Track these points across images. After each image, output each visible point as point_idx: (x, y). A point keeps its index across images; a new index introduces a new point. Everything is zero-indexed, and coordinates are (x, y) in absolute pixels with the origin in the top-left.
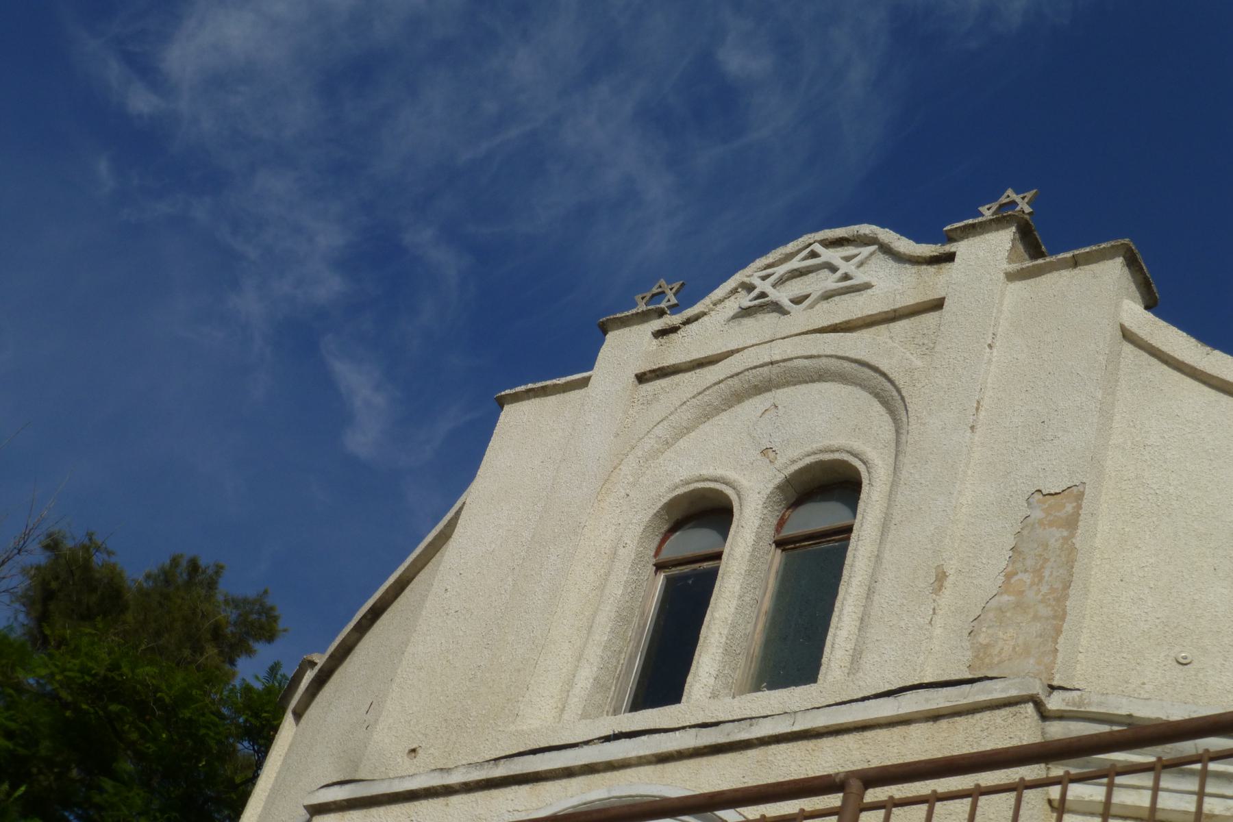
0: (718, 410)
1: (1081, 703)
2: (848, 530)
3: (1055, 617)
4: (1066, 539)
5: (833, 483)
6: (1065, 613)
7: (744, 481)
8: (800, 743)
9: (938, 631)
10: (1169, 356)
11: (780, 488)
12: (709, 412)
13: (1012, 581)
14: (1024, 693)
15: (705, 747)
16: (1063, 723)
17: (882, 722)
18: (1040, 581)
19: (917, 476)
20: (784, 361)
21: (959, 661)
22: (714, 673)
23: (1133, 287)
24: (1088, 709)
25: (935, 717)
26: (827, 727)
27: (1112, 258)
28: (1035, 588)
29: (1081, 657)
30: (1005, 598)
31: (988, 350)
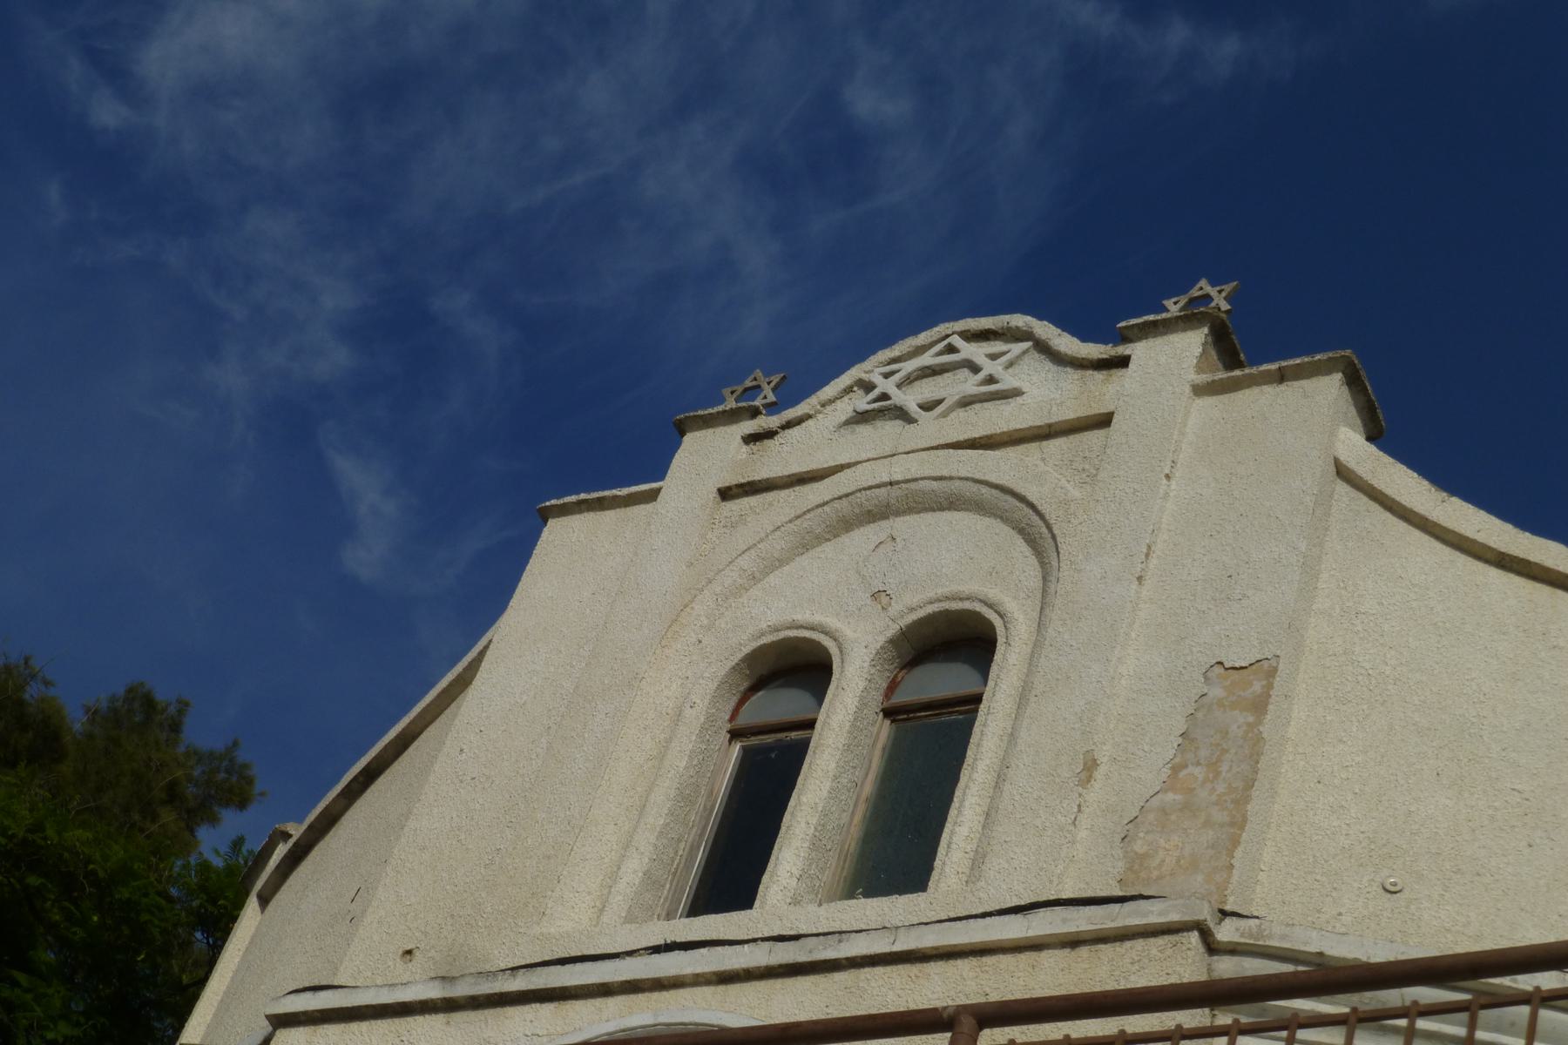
0: (820, 540)
2: (977, 699)
3: (1232, 824)
6: (1245, 820)
7: (848, 631)
8: (900, 967)
9: (1083, 834)
10: (1393, 500)
11: (892, 641)
12: (807, 543)
13: (1182, 774)
14: (1187, 918)
15: (781, 966)
16: (1236, 959)
22: (797, 873)
23: (1353, 411)
24: (1268, 943)
25: (1073, 942)
27: (1329, 372)
29: (1262, 876)
30: (1170, 796)
31: (1165, 481)
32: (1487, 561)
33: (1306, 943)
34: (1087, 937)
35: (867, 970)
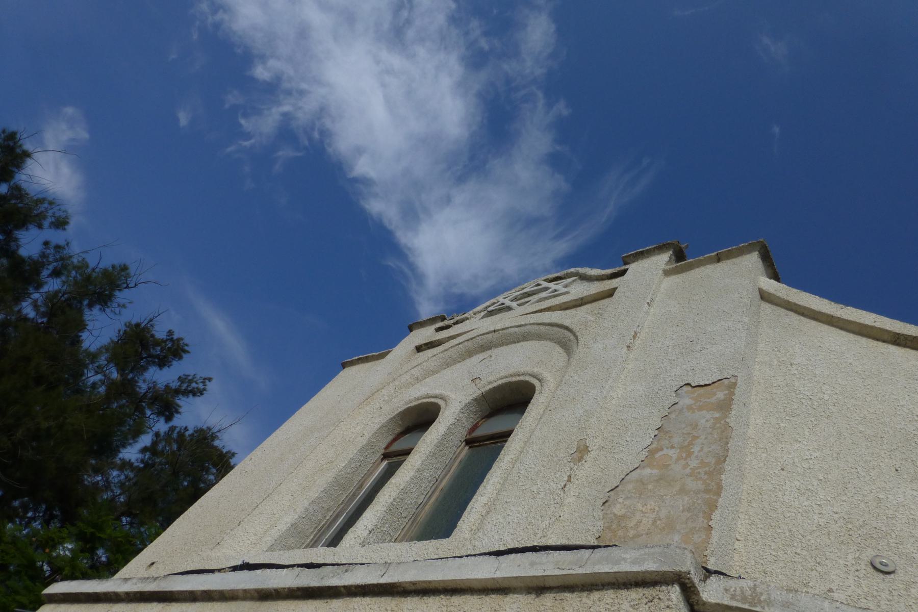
0: (455, 361)
3: (707, 491)
8: (383, 599)
12: (447, 364)
13: (657, 456)
14: (666, 568)
15: (299, 589)
19: (576, 378)
20: (503, 329)
21: (588, 531)
25: (539, 588)
26: (414, 583)
27: (750, 252)
28: (683, 462)
30: (648, 471)
34: (552, 584)
35: (358, 599)
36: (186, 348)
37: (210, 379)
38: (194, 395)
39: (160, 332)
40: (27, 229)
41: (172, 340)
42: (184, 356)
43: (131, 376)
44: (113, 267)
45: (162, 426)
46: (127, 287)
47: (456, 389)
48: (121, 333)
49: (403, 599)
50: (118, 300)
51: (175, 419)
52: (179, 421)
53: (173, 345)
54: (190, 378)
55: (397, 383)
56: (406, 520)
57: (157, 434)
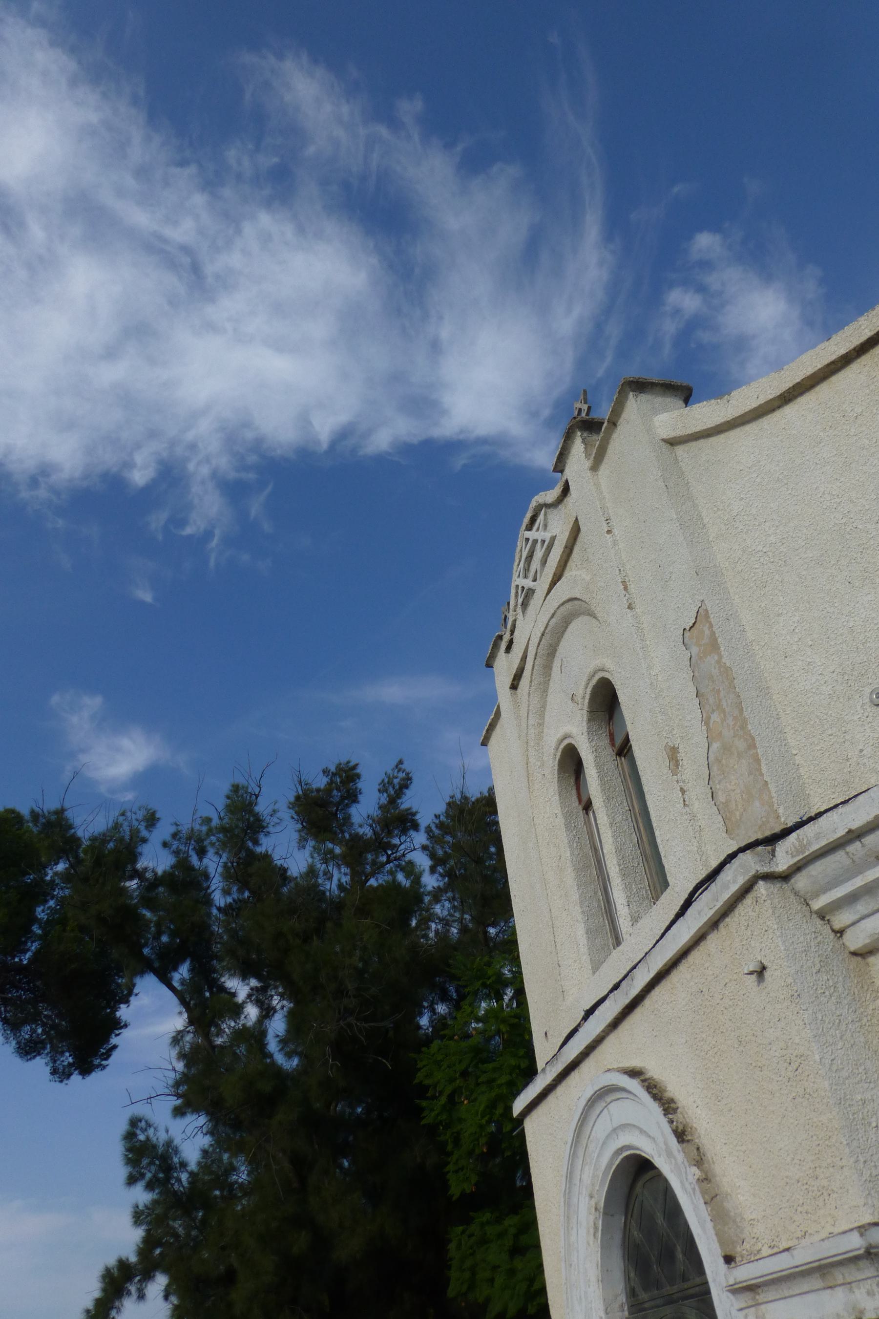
1: (803, 847)
4: (719, 662)
5: (605, 702)
6: (753, 739)
12: (544, 689)
14: (747, 878)
15: (624, 1009)
16: (804, 873)
17: (690, 944)
18: (725, 716)
20: (546, 628)
24: (811, 850)
25: (714, 924)
26: (665, 965)
27: (626, 398)
29: (798, 759)
31: (608, 536)
32: (773, 410)
33: (834, 831)
34: (715, 919)
36: (352, 764)
37: (401, 762)
38: (407, 787)
39: (320, 782)
40: (140, 854)
41: (334, 774)
42: (358, 771)
43: (347, 836)
44: (228, 797)
45: (420, 838)
46: (257, 796)
47: (571, 723)
48: (296, 817)
49: (670, 976)
50: (265, 813)
51: (420, 821)
52: (425, 819)
53: (341, 777)
54: (386, 780)
55: (532, 743)
56: (641, 864)
57: (424, 848)
